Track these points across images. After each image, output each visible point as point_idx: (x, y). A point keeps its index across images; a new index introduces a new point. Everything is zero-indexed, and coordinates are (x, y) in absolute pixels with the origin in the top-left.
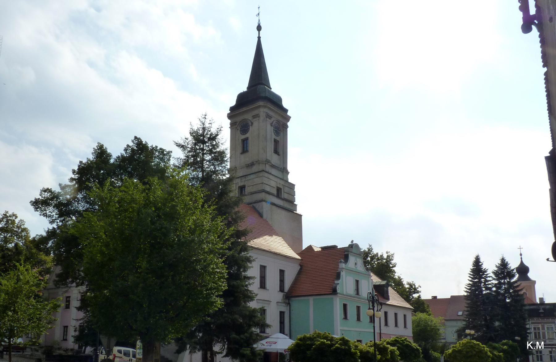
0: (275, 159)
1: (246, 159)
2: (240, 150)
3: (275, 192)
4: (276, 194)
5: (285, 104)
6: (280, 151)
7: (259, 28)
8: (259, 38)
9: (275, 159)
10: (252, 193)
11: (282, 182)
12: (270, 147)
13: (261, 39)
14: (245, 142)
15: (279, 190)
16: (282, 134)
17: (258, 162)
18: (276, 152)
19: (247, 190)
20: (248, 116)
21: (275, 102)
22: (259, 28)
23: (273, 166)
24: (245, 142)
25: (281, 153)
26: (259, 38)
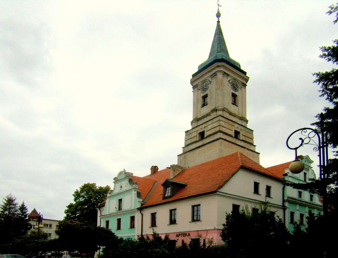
1: (206, 110)
2: (200, 105)
3: (233, 133)
5: (242, 68)
7: (218, 15)
8: (218, 22)
9: (233, 109)
11: (240, 127)
12: (230, 99)
13: (220, 23)
14: (205, 97)
15: (237, 133)
17: (215, 110)
18: (234, 103)
19: (206, 134)
22: (218, 15)
23: (231, 114)
24: (205, 97)
26: (218, 22)
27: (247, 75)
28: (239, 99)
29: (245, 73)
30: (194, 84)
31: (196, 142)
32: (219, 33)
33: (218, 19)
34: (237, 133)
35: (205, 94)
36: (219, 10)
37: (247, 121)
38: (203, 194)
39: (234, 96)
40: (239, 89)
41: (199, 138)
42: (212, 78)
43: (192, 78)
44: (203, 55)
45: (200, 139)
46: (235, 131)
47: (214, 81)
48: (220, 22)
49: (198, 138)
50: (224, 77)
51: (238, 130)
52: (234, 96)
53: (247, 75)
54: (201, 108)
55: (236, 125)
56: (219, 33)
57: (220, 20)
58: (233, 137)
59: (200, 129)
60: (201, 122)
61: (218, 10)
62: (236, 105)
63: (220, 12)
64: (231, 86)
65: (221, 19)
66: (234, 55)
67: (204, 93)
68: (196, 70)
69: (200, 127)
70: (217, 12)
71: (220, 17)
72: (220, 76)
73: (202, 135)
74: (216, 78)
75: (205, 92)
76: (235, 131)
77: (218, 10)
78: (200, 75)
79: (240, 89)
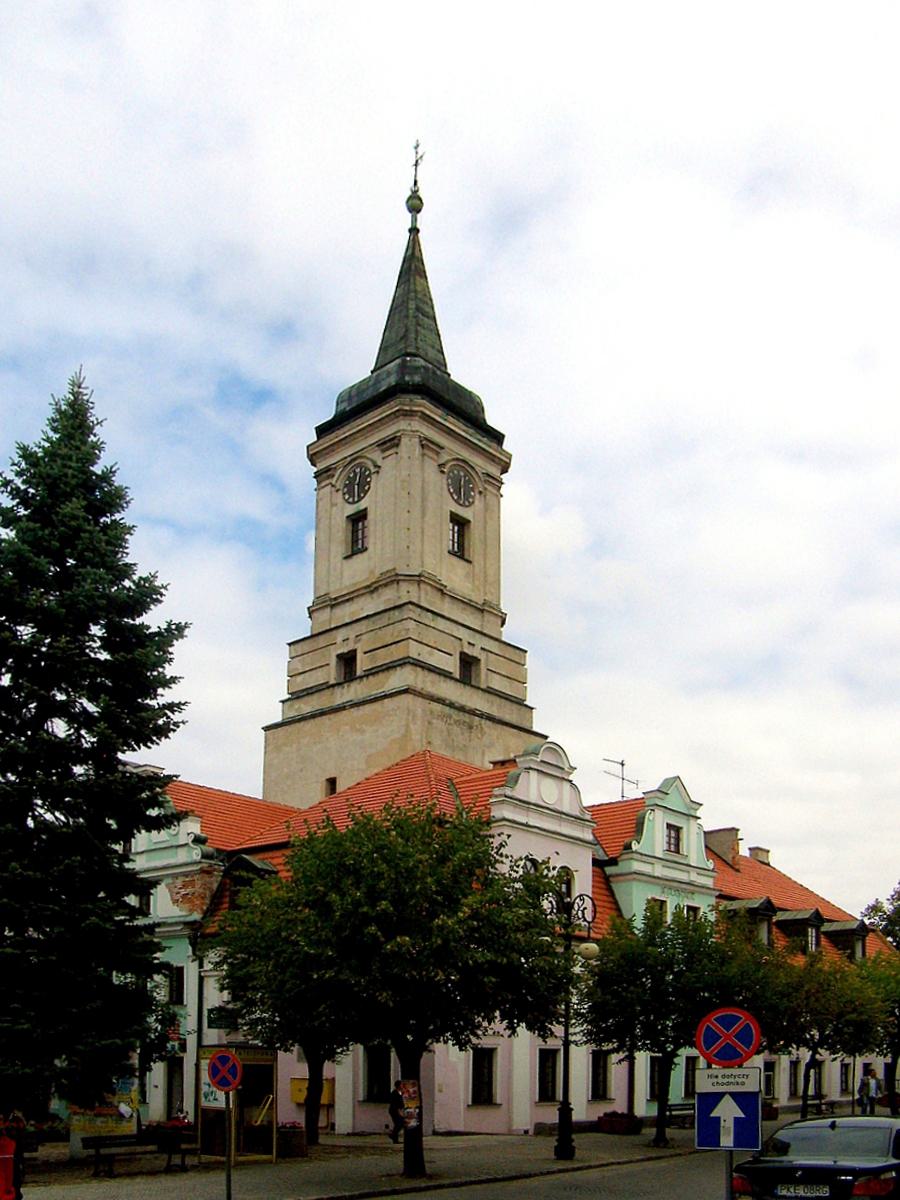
0: (454, 575)
1: (359, 571)
5: (492, 419)
7: (415, 205)
8: (414, 231)
9: (454, 575)
16: (478, 502)
18: (460, 552)
19: (362, 664)
21: (464, 409)
22: (415, 205)
26: (414, 231)
27: (504, 447)
28: (475, 534)
29: (498, 438)
30: (322, 465)
32: (412, 267)
33: (414, 220)
36: (419, 184)
39: (460, 523)
40: (478, 496)
41: (339, 674)
44: (355, 354)
45: (342, 680)
47: (388, 465)
48: (418, 231)
49: (332, 674)
50: (423, 455)
52: (460, 523)
53: (507, 446)
54: (344, 561)
55: (462, 633)
56: (412, 267)
57: (418, 226)
60: (345, 613)
62: (466, 557)
63: (421, 194)
64: (448, 485)
65: (423, 219)
66: (463, 368)
69: (340, 635)
70: (409, 193)
71: (419, 211)
72: (409, 447)
73: (348, 660)
74: (397, 453)
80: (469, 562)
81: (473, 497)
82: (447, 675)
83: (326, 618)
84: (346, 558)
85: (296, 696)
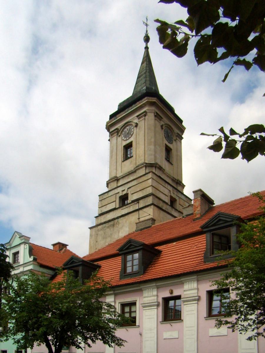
1: (129, 166)
3: (167, 200)
4: (169, 204)
6: (174, 160)
8: (147, 48)
10: (137, 200)
13: (149, 50)
14: (128, 147)
15: (173, 201)
19: (131, 198)
20: (133, 119)
25: (174, 163)
26: (147, 48)
31: (115, 209)
34: (173, 201)
35: (128, 142)
36: (148, 32)
37: (183, 186)
38: (121, 285)
39: (168, 150)
42: (139, 119)
43: (109, 120)
45: (121, 206)
46: (171, 197)
51: (174, 196)
52: (168, 150)
58: (168, 205)
59: (121, 192)
61: (147, 31)
62: (170, 161)
65: (149, 45)
67: (126, 140)
68: (116, 109)
70: (144, 35)
73: (124, 199)
75: (127, 138)
76: (171, 197)
77: (147, 31)
78: (123, 114)
79: (175, 140)
80: (172, 164)
81: (173, 141)
82: (167, 204)
83: (114, 185)
84: (123, 162)
85: (101, 215)
